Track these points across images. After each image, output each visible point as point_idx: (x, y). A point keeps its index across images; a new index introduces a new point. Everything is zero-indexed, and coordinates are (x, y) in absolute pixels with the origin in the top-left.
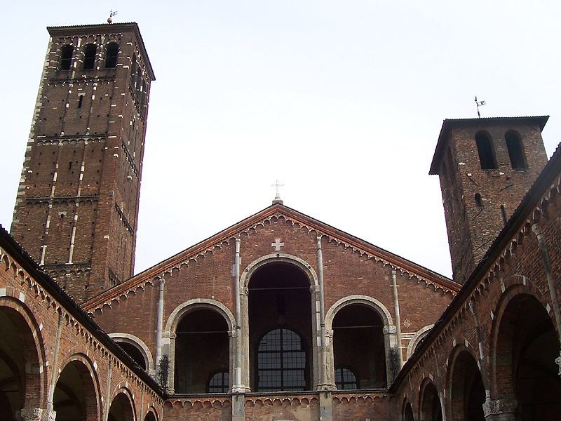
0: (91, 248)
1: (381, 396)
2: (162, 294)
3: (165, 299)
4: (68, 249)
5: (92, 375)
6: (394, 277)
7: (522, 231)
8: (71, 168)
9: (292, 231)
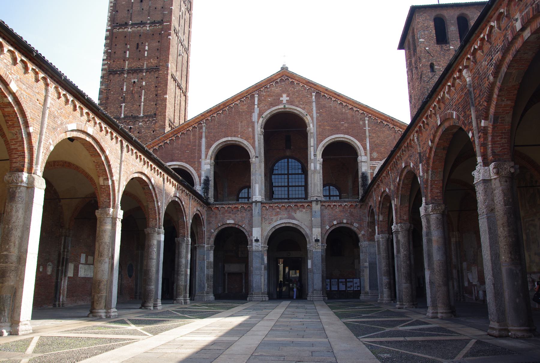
0: (156, 104)
1: (354, 204)
2: (204, 135)
3: (206, 138)
4: (140, 106)
5: (150, 187)
6: (367, 122)
7: (455, 76)
9: (294, 89)
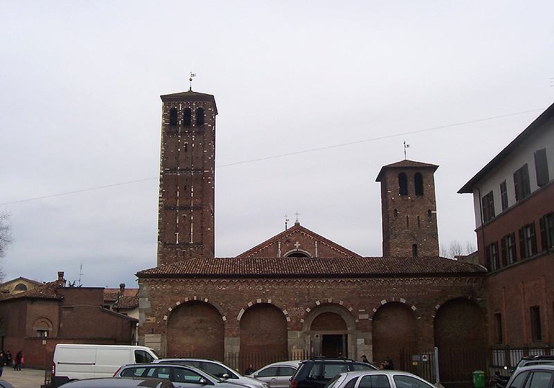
8: (186, 189)
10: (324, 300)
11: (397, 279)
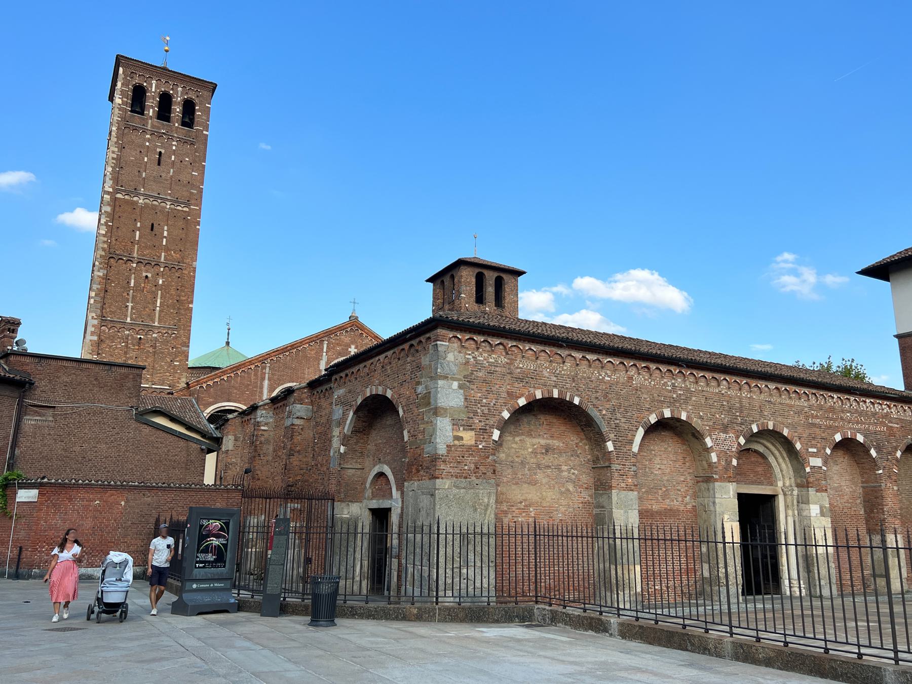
4: (154, 310)
10: (763, 423)
11: (852, 398)
